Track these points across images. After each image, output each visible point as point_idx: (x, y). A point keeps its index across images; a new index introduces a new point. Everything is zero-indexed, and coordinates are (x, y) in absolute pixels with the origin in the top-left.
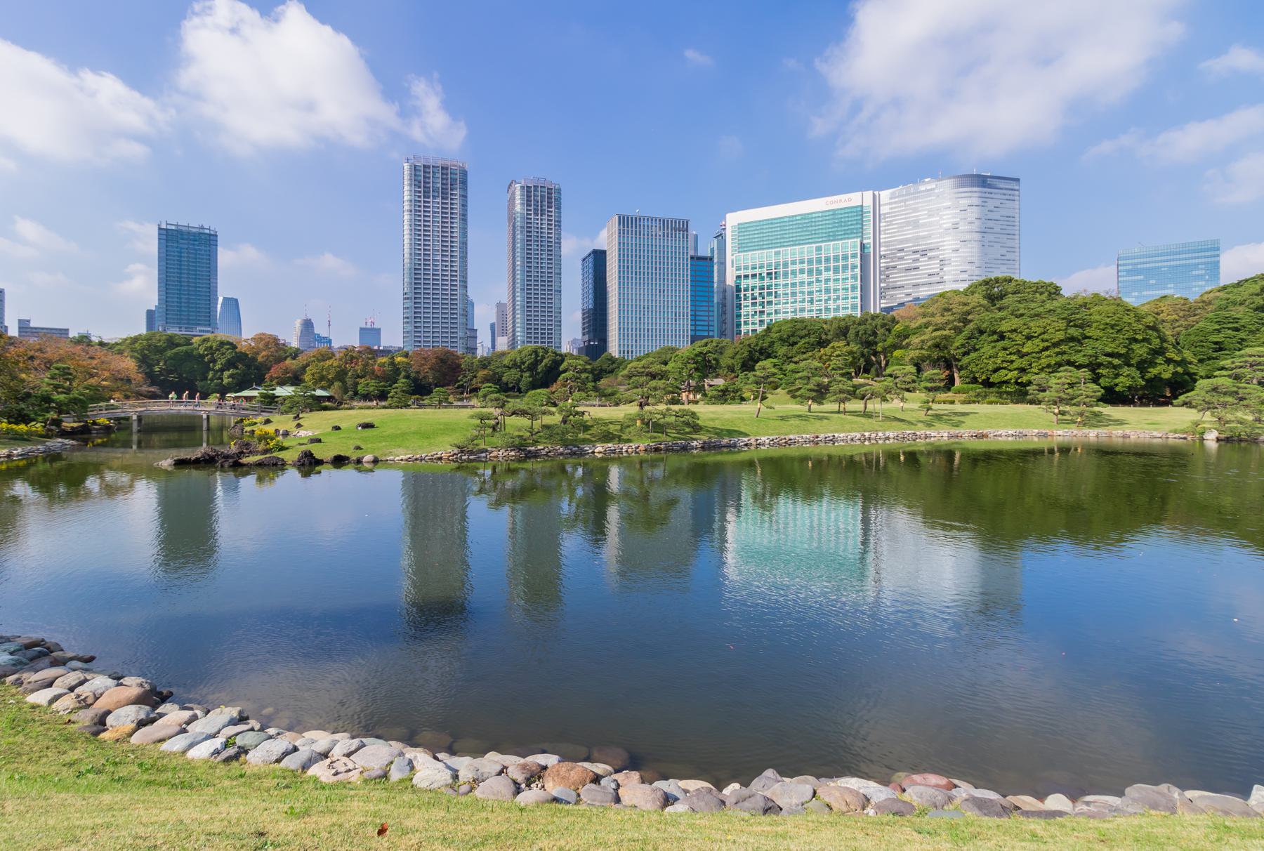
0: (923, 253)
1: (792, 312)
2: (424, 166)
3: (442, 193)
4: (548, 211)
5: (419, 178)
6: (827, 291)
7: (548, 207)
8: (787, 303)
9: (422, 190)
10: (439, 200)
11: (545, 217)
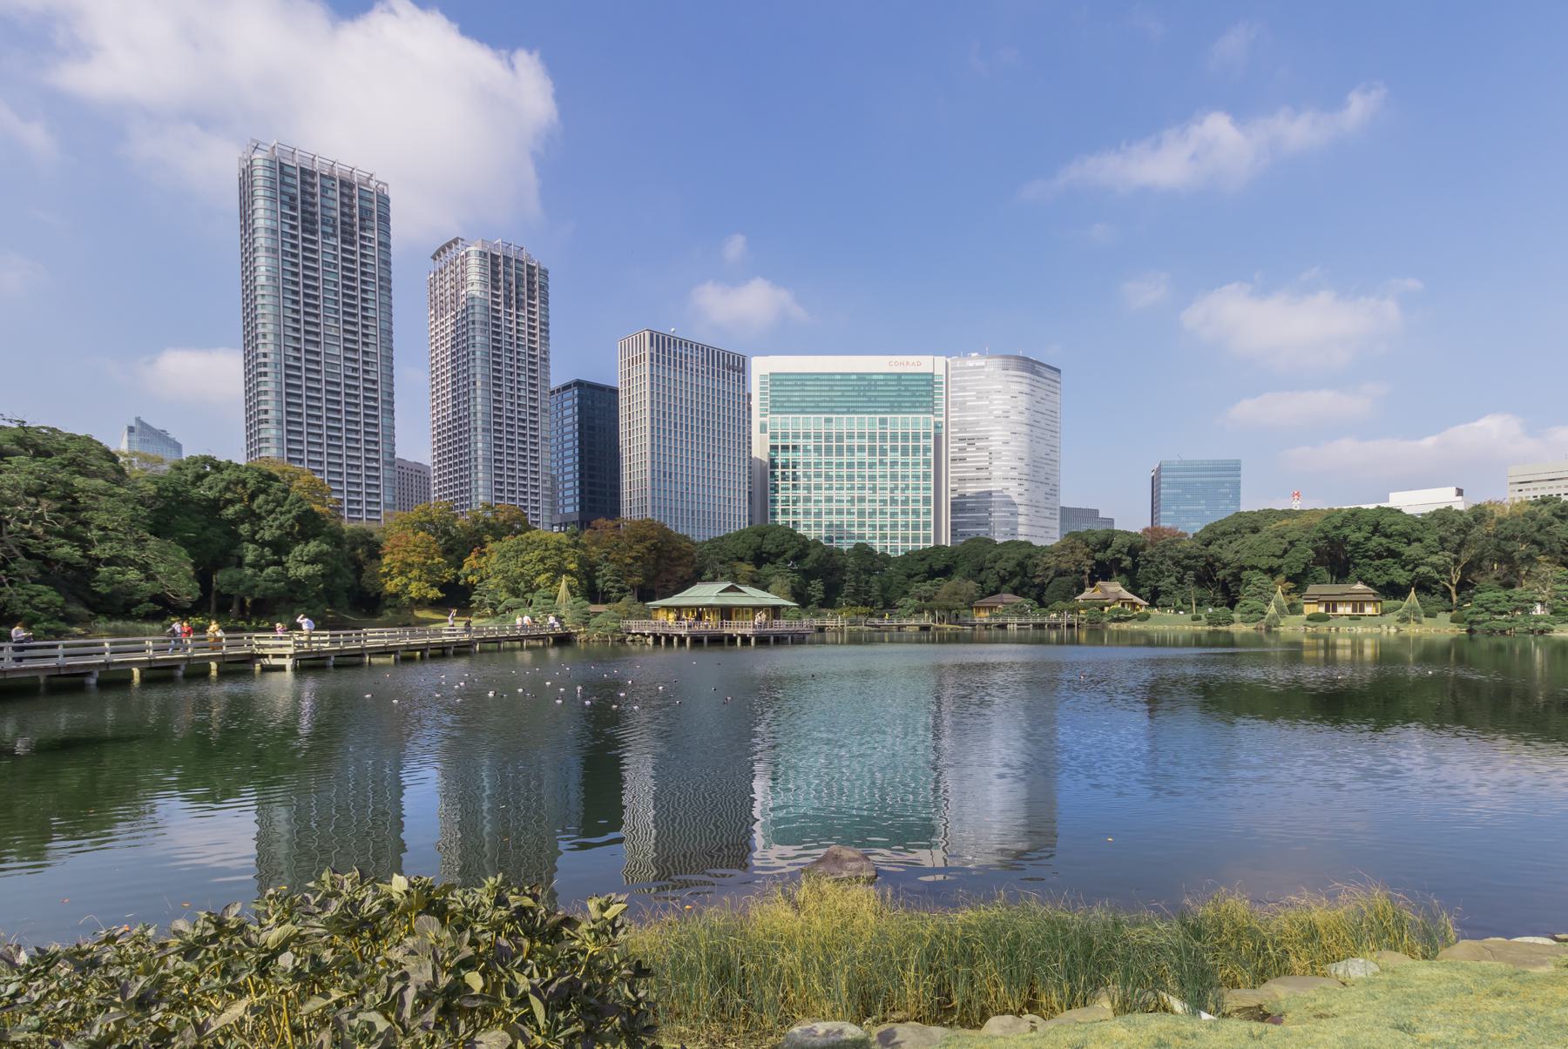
0: (970, 442)
1: (848, 501)
2: (303, 171)
3: (343, 232)
7: (529, 298)
8: (842, 489)
9: (298, 214)
10: (336, 241)
11: (524, 313)
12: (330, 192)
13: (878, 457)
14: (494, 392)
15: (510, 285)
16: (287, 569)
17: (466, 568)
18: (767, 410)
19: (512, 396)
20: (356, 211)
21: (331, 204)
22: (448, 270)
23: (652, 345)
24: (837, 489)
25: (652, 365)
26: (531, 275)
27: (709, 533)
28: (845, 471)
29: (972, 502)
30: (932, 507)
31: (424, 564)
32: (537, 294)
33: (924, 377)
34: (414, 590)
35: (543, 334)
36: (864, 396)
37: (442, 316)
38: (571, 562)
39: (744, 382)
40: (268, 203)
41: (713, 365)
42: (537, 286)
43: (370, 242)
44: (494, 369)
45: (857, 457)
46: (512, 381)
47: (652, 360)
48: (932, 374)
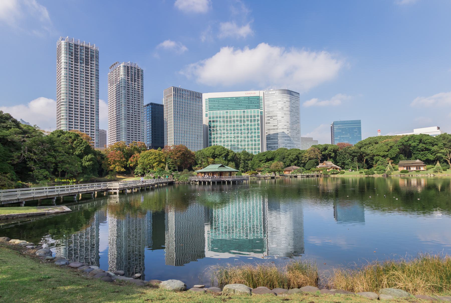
1: (233, 137)
2: (75, 45)
3: (86, 62)
4: (138, 81)
5: (72, 51)
6: (248, 129)
7: (138, 79)
8: (231, 133)
9: (73, 57)
10: (84, 65)
11: (136, 83)
12: (82, 50)
13: (243, 123)
14: (127, 107)
15: (132, 75)
16: (82, 163)
17: (129, 162)
18: (207, 110)
19: (132, 108)
20: (89, 56)
21: (83, 54)
22: (114, 71)
23: (174, 91)
24: (230, 134)
25: (174, 97)
26: (138, 72)
27: (198, 149)
28: (232, 128)
29: (272, 137)
30: (260, 139)
31: (120, 161)
32: (140, 77)
33: (256, 97)
34: (117, 169)
35: (142, 89)
36: (238, 104)
37: (112, 85)
38: (163, 159)
39: (201, 101)
40: (65, 55)
41: (192, 96)
42: (140, 75)
43: (93, 64)
44: (127, 101)
45: (236, 123)
46: (132, 104)
47: (174, 96)
48: (259, 96)
